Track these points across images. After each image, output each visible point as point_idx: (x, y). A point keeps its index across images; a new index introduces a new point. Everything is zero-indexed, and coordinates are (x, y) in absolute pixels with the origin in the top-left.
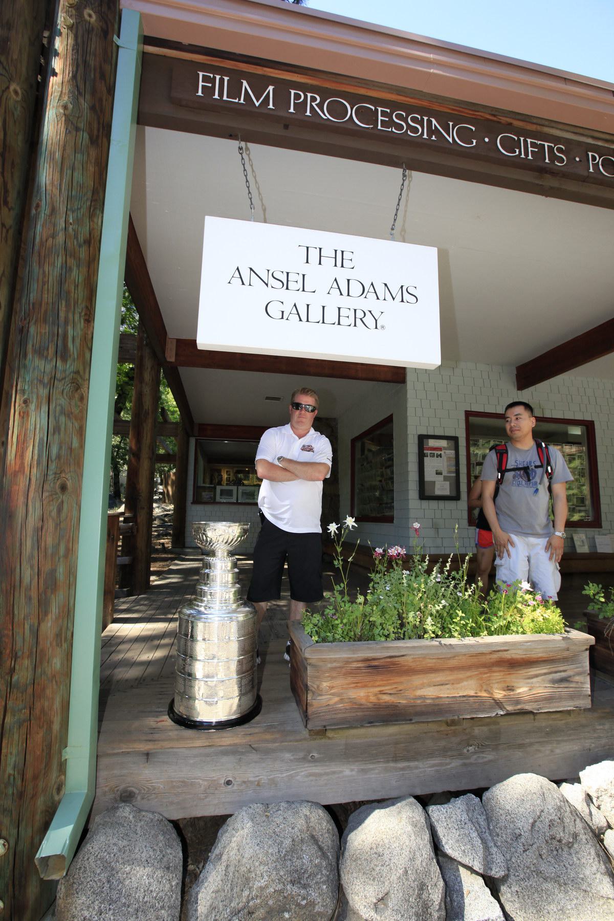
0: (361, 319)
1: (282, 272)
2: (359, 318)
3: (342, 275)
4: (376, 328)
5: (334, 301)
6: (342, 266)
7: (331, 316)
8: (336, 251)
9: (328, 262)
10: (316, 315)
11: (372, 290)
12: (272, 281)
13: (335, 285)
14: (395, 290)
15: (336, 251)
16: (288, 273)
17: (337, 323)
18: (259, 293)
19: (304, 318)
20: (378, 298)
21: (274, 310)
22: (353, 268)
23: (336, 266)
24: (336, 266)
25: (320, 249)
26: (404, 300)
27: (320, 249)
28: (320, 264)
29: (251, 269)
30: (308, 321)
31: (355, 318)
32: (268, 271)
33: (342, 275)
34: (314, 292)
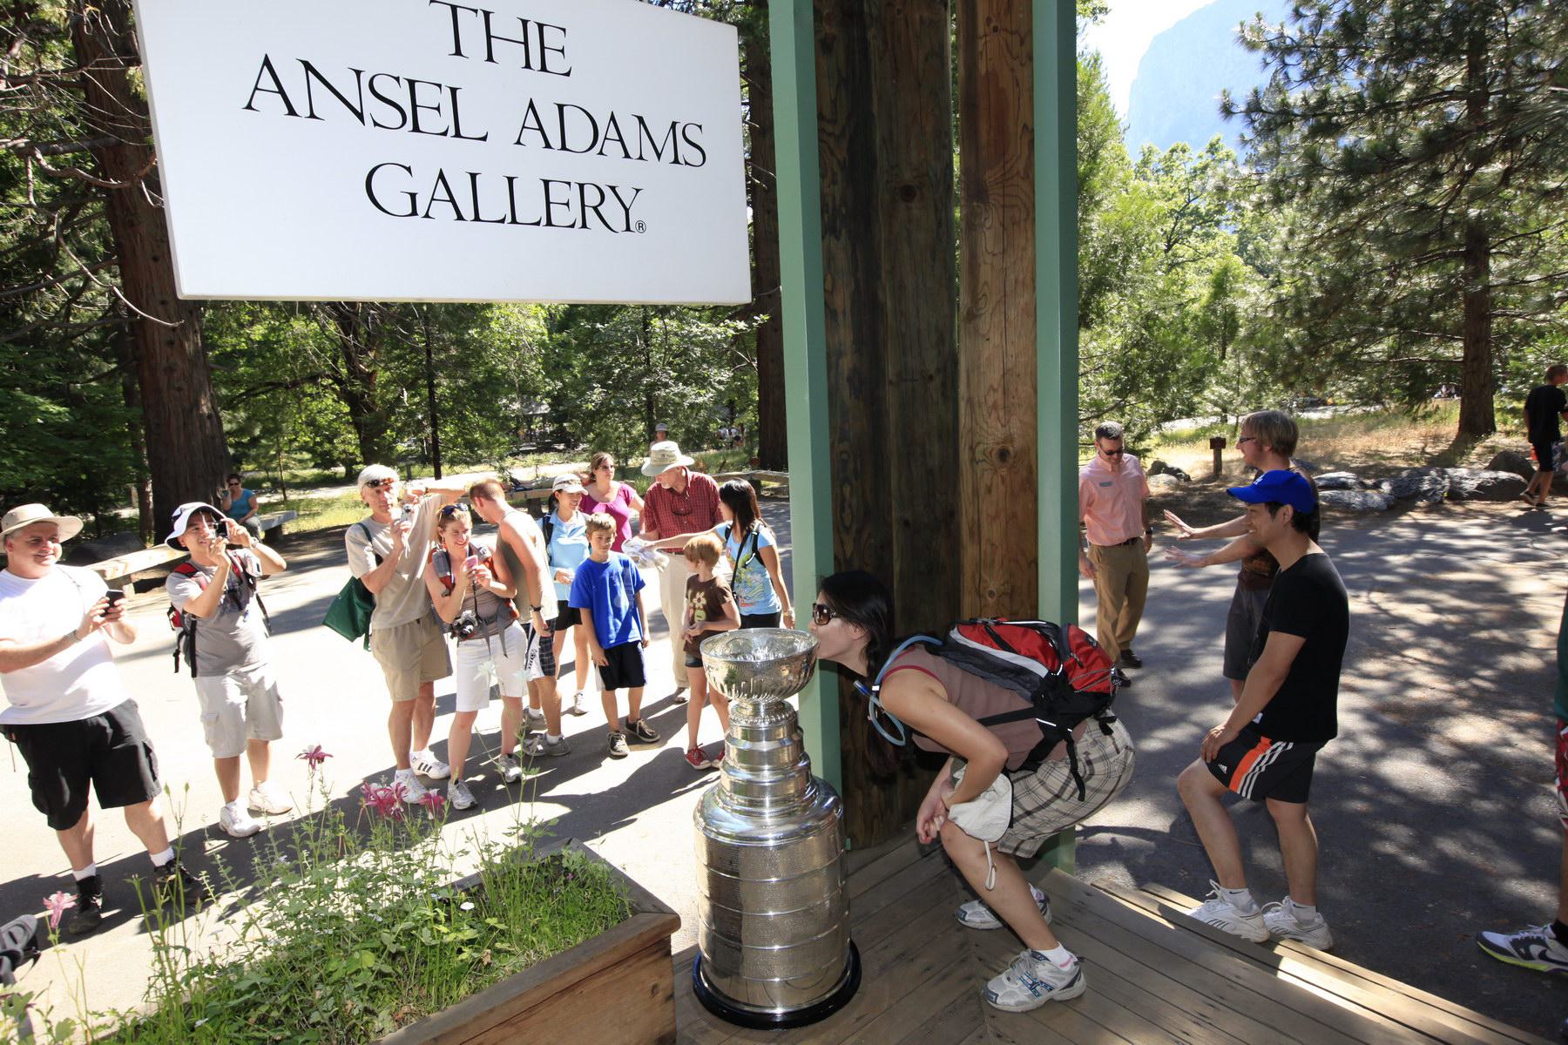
0: (595, 208)
1: (397, 79)
3: (547, 92)
4: (628, 229)
5: (534, 163)
6: (544, 68)
7: (530, 205)
8: (525, 23)
9: (509, 54)
10: (494, 202)
11: (613, 134)
12: (372, 106)
13: (532, 122)
14: (660, 133)
15: (525, 23)
16: (412, 83)
17: (544, 222)
19: (468, 212)
20: (627, 156)
21: (390, 187)
22: (568, 74)
23: (528, 66)
24: (528, 66)
25: (487, 14)
26: (681, 160)
27: (487, 14)
28: (490, 59)
29: (308, 66)
30: (477, 218)
31: (583, 206)
32: (358, 73)
33: (547, 92)
34: (484, 139)
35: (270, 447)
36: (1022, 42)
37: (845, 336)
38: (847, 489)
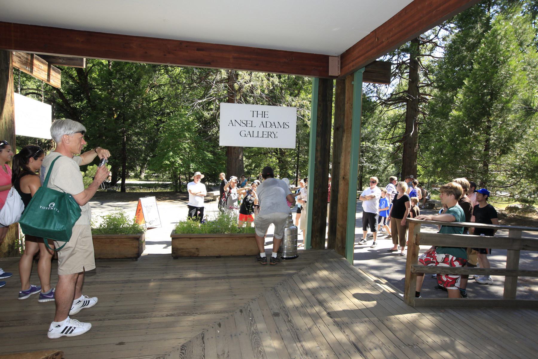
2: (269, 135)
3: (264, 120)
5: (262, 129)
7: (260, 135)
10: (255, 134)
12: (242, 124)
14: (281, 124)
18: (238, 128)
33: (264, 120)
35: (257, 170)
36: (351, 105)
37: (319, 154)
38: (317, 181)
